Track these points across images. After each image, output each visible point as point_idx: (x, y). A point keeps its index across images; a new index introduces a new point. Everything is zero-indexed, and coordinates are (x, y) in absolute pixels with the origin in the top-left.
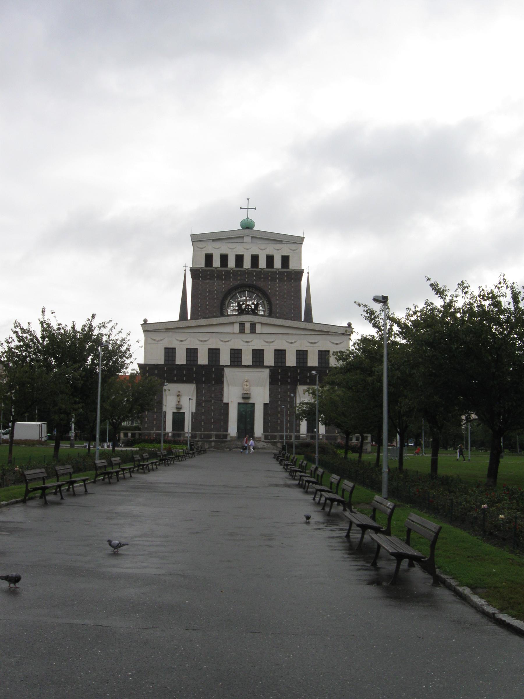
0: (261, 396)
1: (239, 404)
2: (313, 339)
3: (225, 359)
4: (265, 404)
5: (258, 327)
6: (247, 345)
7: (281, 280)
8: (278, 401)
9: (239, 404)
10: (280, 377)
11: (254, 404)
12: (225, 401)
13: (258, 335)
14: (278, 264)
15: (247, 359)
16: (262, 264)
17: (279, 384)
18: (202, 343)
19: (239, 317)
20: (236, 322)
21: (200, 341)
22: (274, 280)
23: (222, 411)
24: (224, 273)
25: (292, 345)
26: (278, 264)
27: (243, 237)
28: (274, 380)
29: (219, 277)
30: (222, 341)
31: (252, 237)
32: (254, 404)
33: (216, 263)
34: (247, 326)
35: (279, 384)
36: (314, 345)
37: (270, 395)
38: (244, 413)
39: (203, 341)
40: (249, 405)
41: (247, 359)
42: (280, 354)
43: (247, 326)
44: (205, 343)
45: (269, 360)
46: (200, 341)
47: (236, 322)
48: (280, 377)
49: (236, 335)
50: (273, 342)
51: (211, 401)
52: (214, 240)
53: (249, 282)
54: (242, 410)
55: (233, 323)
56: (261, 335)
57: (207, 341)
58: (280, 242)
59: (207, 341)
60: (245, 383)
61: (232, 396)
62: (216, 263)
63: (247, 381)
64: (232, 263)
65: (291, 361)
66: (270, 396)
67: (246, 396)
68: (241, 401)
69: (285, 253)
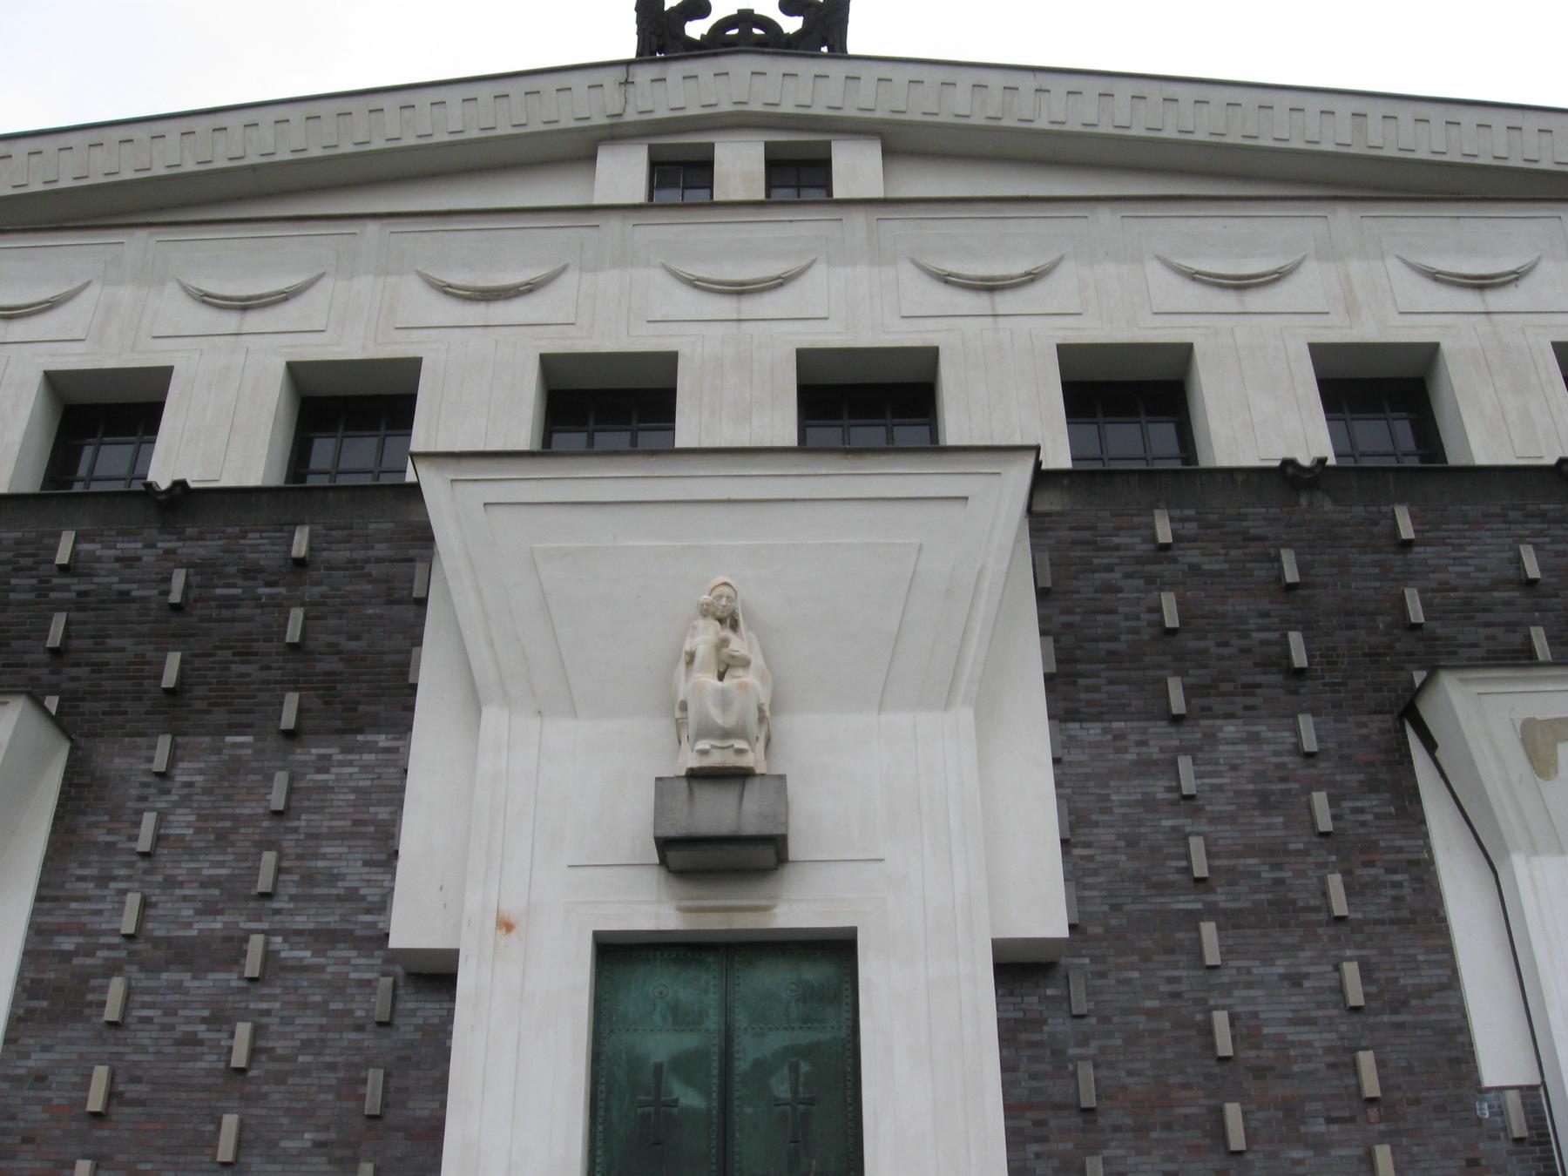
0: (942, 838)
1: (615, 954)
8: (1192, 920)
9: (615, 954)
10: (1169, 601)
11: (838, 949)
12: (411, 927)
13: (858, 221)
17: (1178, 704)
18: (230, 321)
19: (644, 74)
20: (617, 133)
21: (207, 299)
23: (375, 1077)
25: (1255, 300)
28: (1090, 669)
30: (446, 290)
32: (838, 949)
34: (739, 165)
35: (1178, 704)
36: (1494, 299)
37: (1064, 842)
38: (689, 1098)
39: (245, 305)
40: (773, 978)
42: (1126, 393)
43: (739, 165)
44: (254, 320)
46: (207, 299)
47: (617, 133)
48: (1169, 601)
49: (614, 226)
50: (1032, 278)
51: (231, 950)
54: (661, 1045)
56: (898, 229)
57: (285, 297)
59: (285, 297)
60: (704, 637)
61: (512, 845)
63: (730, 621)
67: (716, 813)
68: (653, 909)
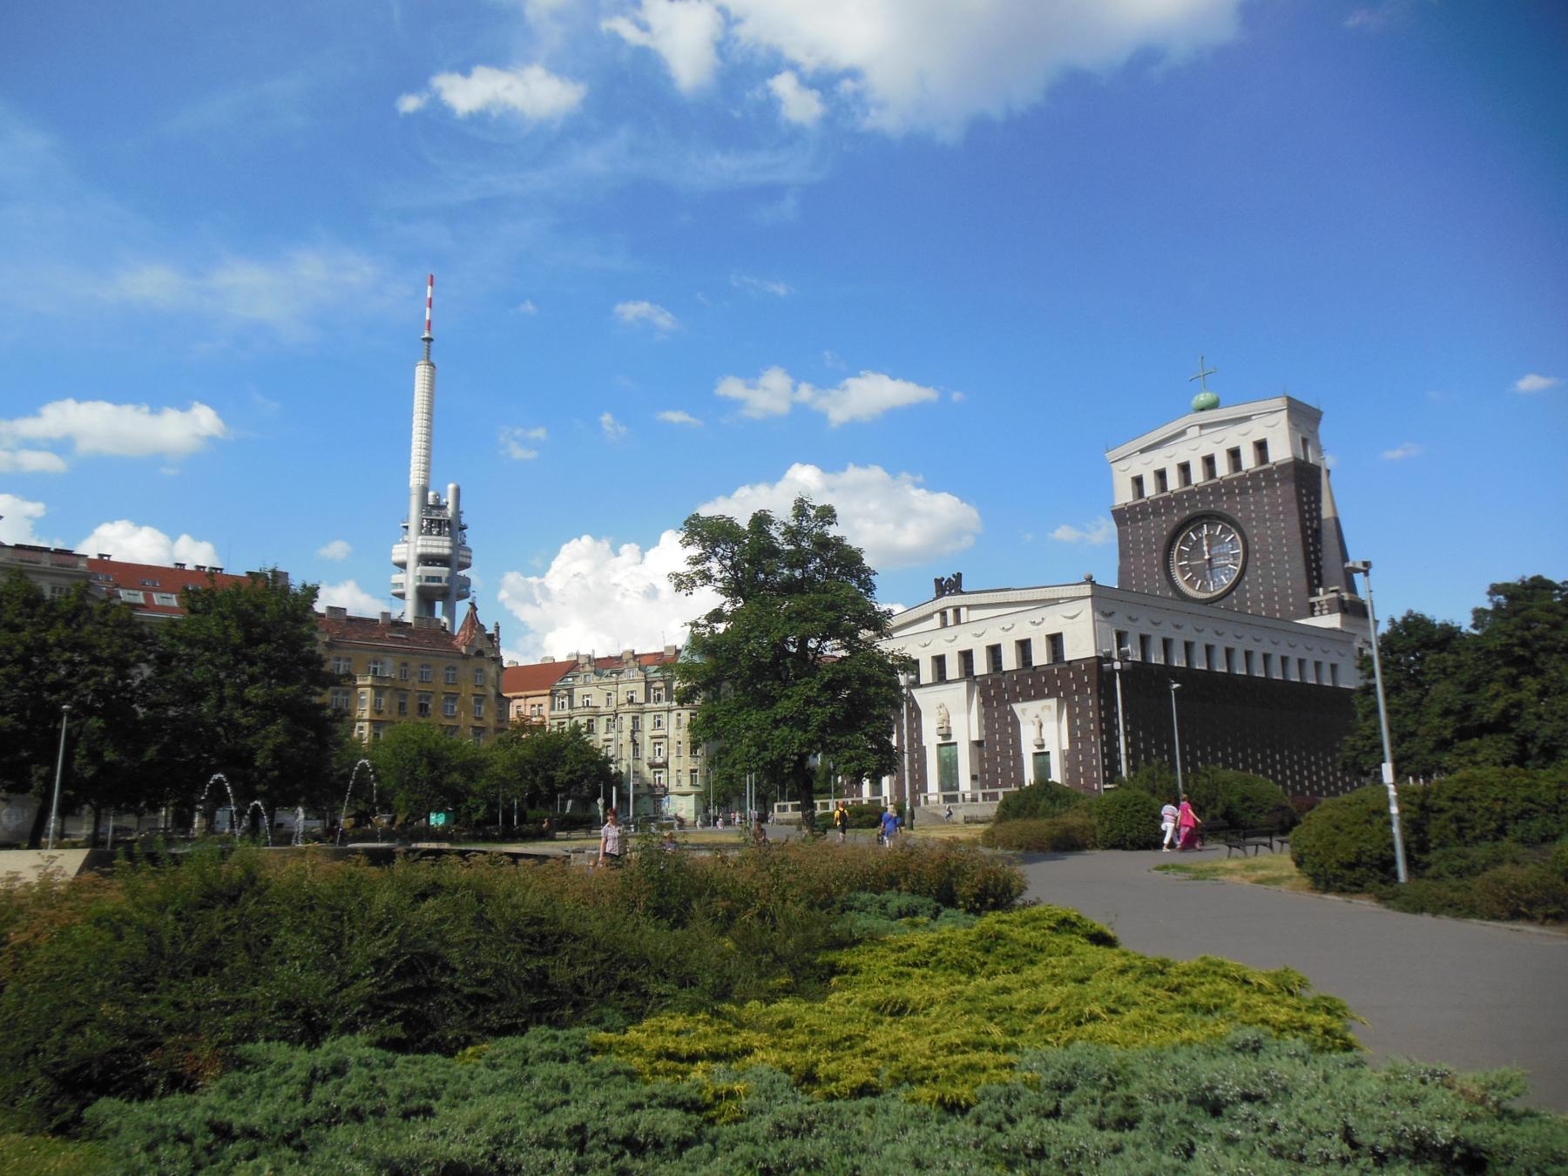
0: (967, 727)
2: (1037, 615)
3: (926, 674)
4: (979, 744)
5: (963, 610)
6: (949, 644)
7: (1257, 488)
14: (1249, 461)
15: (953, 670)
16: (1223, 469)
22: (1243, 492)
24: (1167, 503)
26: (1249, 461)
27: (1183, 433)
29: (1156, 513)
31: (1202, 427)
33: (1150, 490)
34: (950, 613)
41: (953, 670)
43: (950, 613)
45: (981, 666)
52: (1142, 451)
53: (1206, 508)
55: (929, 616)
58: (1247, 419)
62: (1150, 490)
64: (1173, 483)
65: (1010, 662)
66: (986, 727)
69: (1259, 438)
